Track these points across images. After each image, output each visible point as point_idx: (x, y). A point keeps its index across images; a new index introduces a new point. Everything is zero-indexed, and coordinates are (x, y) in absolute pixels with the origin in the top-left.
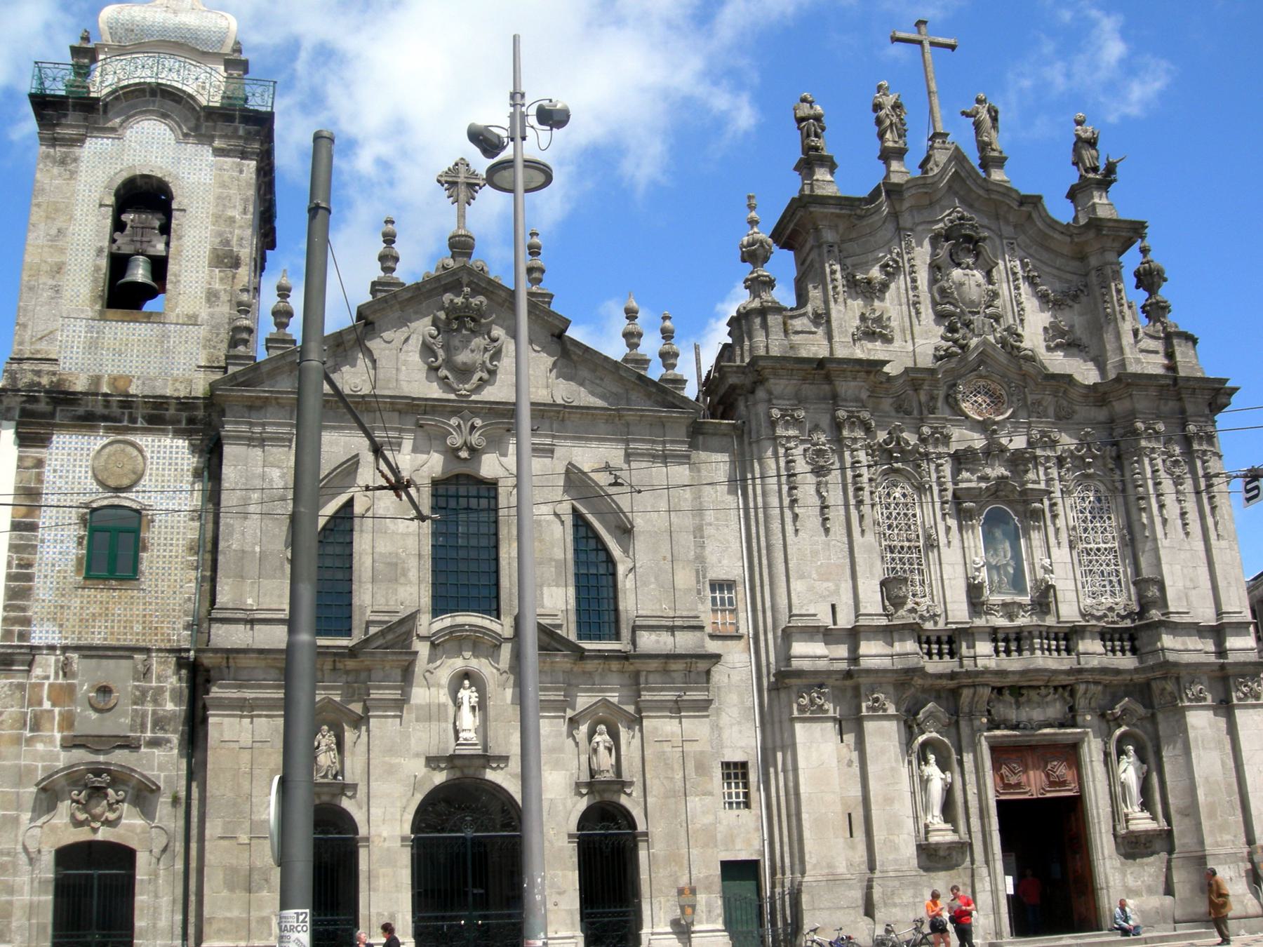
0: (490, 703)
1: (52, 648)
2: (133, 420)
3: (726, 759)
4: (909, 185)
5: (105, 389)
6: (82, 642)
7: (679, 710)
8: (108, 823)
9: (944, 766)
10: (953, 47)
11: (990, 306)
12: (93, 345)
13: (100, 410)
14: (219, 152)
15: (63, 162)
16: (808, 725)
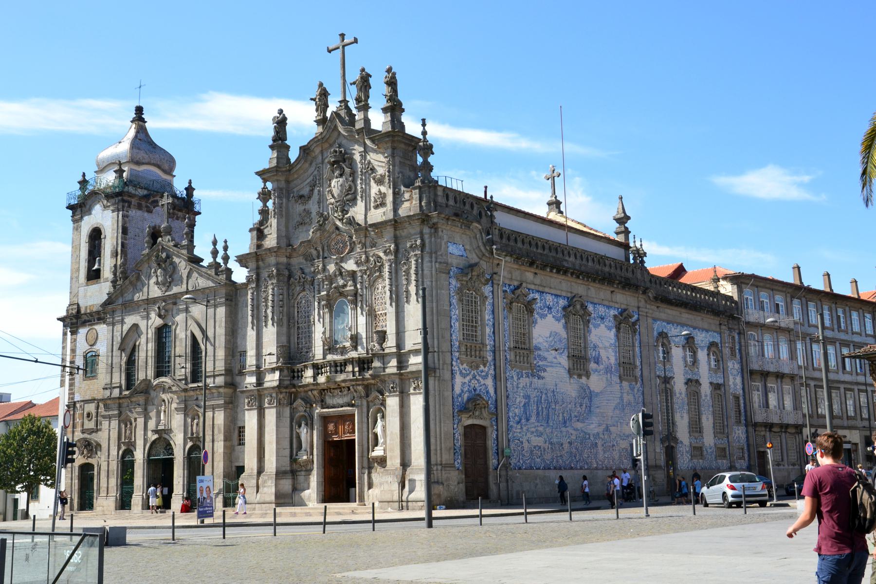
0: (167, 410)
1: (78, 401)
2: (94, 321)
3: (239, 426)
4: (311, 143)
5: (88, 311)
6: (84, 399)
7: (216, 408)
8: (88, 457)
9: (306, 424)
10: (356, 41)
11: (349, 194)
12: (85, 296)
13: (87, 318)
14: (113, 211)
15: (77, 229)
16: (249, 411)
